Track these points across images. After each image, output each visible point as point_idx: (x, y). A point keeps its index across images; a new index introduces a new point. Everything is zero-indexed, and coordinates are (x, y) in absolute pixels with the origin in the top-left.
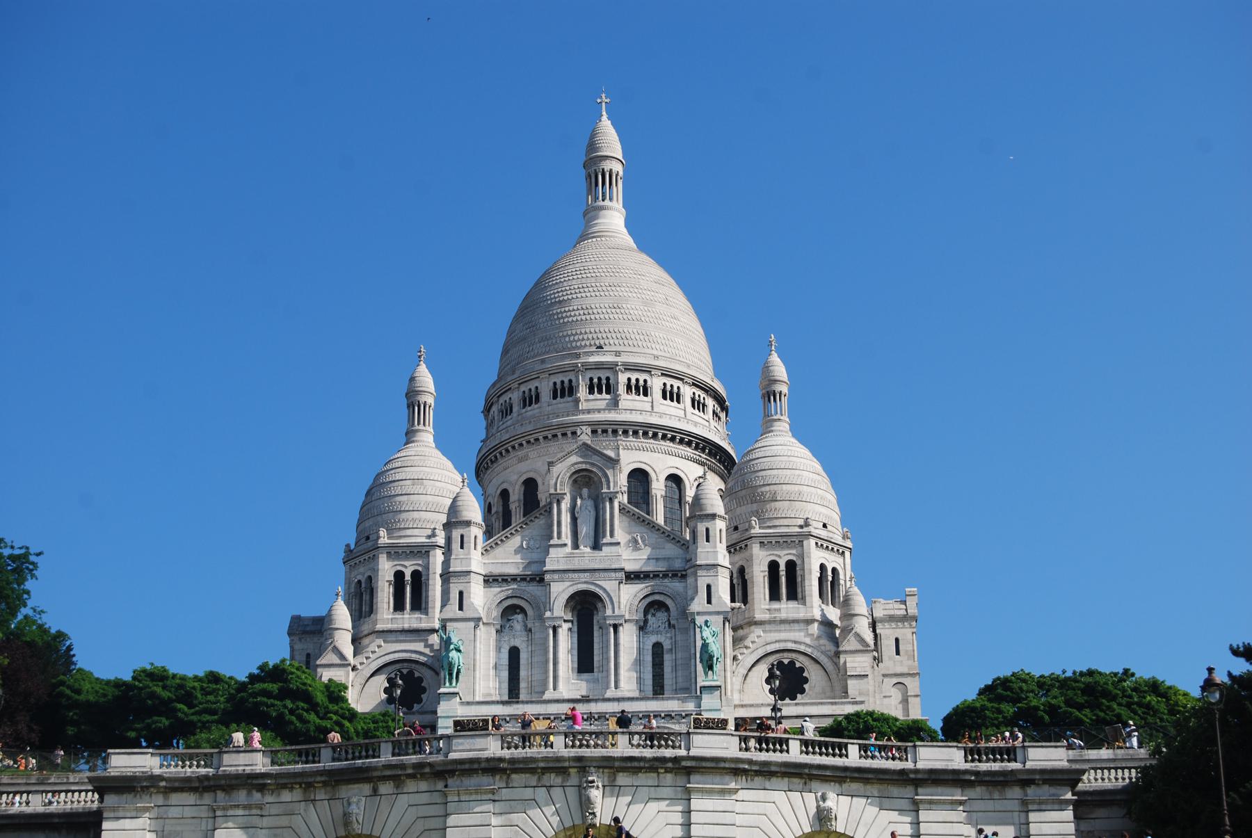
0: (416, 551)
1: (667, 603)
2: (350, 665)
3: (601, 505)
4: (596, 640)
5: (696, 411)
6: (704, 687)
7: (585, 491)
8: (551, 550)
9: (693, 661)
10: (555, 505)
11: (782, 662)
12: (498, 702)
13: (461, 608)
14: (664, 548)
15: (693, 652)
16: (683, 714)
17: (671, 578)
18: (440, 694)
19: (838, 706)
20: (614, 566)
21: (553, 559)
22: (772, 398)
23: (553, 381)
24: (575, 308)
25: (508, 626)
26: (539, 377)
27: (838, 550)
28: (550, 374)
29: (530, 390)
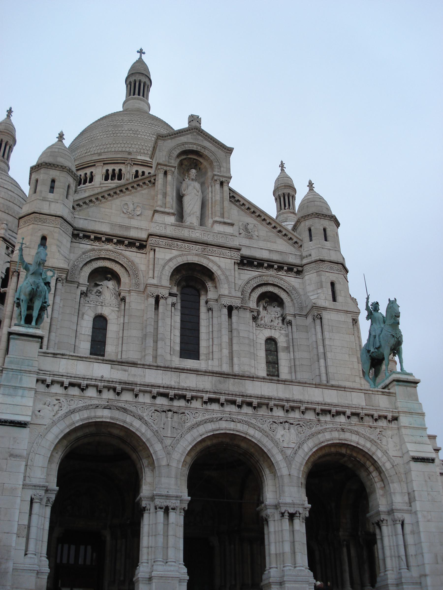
3: (210, 188)
4: (203, 323)
6: (398, 381)
7: (193, 171)
8: (156, 215)
9: (322, 361)
10: (161, 176)
14: (275, 242)
15: (321, 350)
17: (285, 271)
18: (10, 334)
21: (160, 225)
23: (106, 168)
24: (126, 129)
26: (95, 165)
28: (104, 164)
29: (86, 174)
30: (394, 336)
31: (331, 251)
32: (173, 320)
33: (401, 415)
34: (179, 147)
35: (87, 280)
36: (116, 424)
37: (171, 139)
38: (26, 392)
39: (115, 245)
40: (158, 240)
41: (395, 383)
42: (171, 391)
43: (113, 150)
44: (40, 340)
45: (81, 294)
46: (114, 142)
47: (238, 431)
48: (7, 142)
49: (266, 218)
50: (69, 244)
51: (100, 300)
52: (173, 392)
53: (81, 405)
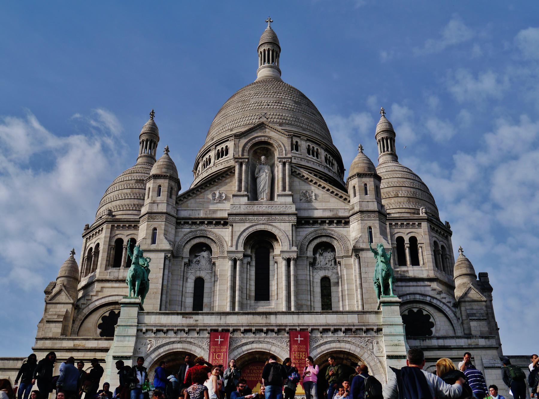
0: (133, 225)
1: (333, 244)
2: (73, 304)
5: (328, 166)
7: (263, 158)
8: (235, 198)
11: (412, 310)
12: (178, 314)
13: (154, 242)
14: (329, 202)
16: (364, 328)
19: (473, 340)
20: (287, 212)
21: (236, 206)
22: (385, 141)
24: (252, 103)
25: (195, 260)
27: (444, 234)
29: (223, 148)
30: (384, 270)
31: (370, 203)
32: (248, 275)
33: (384, 327)
34: (251, 142)
35: (188, 254)
36: (186, 352)
37: (245, 136)
38: (131, 338)
39: (206, 226)
40: (235, 217)
41: (381, 304)
42: (219, 328)
43: (242, 123)
44: (138, 305)
45: (185, 264)
46: (243, 117)
47: (264, 349)
48: (152, 140)
49: (321, 183)
50: (173, 232)
51: (199, 267)
52: (221, 328)
53: (164, 342)
